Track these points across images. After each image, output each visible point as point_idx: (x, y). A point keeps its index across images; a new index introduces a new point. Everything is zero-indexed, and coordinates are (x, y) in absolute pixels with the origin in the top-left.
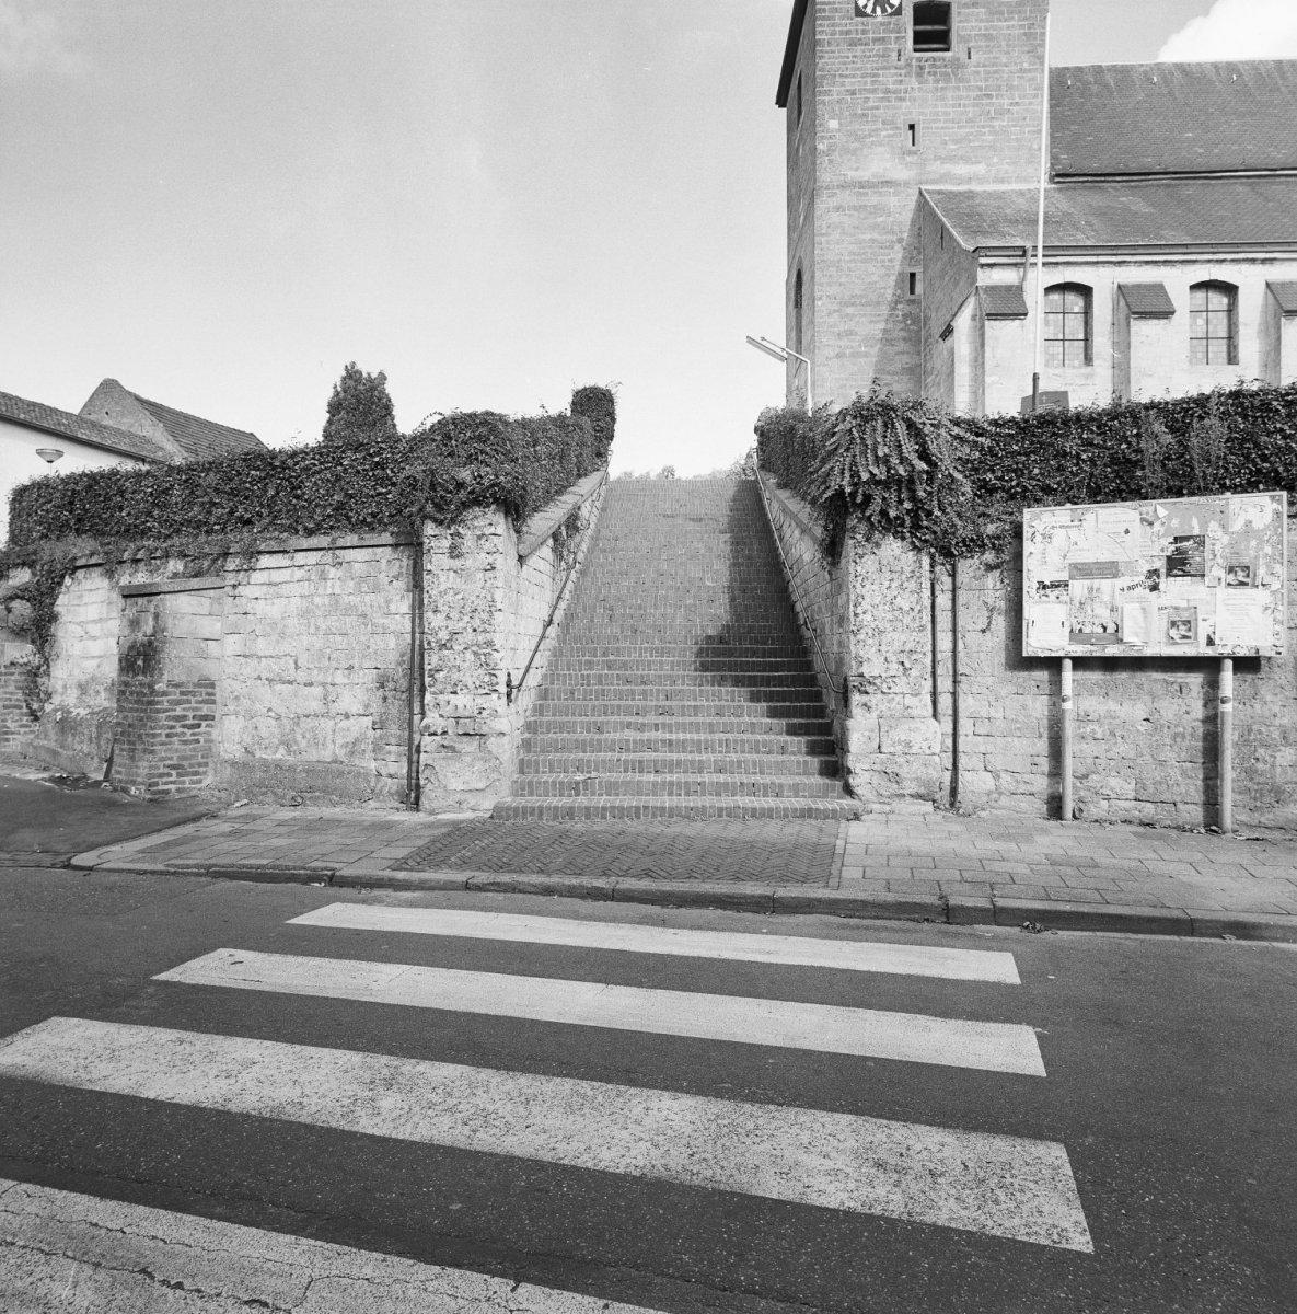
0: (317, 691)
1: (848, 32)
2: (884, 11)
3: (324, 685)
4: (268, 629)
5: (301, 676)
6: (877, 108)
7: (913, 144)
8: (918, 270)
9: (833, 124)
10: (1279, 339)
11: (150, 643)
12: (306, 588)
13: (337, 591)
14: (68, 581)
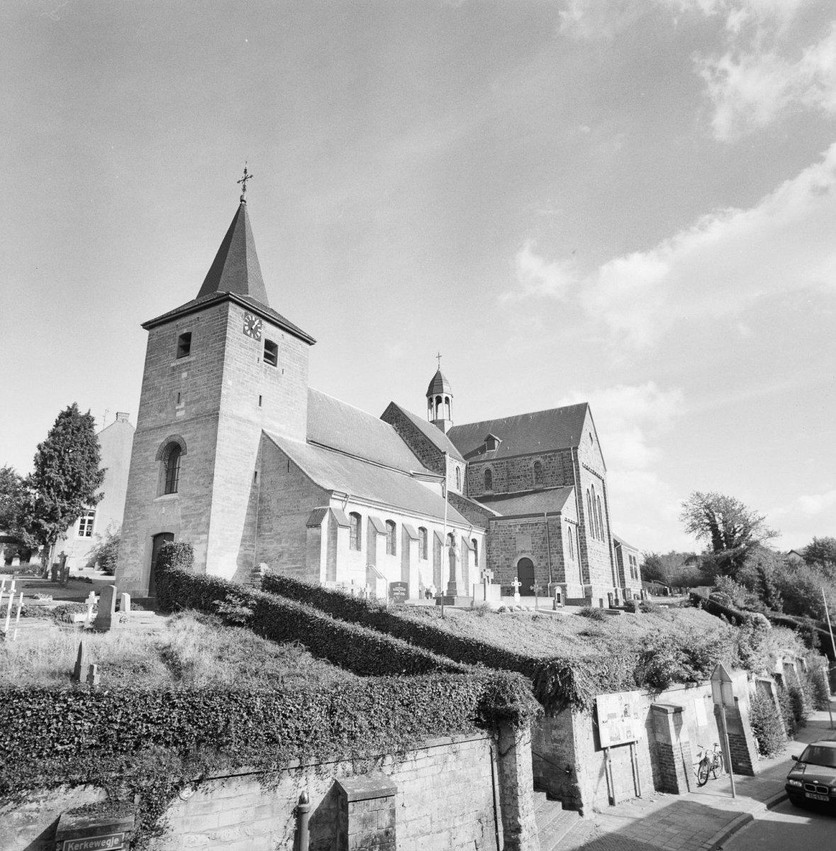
0: (445, 834)
1: (240, 339)
2: (254, 337)
3: (449, 829)
4: (412, 800)
5: (436, 827)
6: (247, 382)
7: (260, 405)
8: (259, 472)
9: (230, 383)
10: (409, 548)
11: (387, 833)
12: (436, 770)
13: (454, 768)
14: (186, 793)
